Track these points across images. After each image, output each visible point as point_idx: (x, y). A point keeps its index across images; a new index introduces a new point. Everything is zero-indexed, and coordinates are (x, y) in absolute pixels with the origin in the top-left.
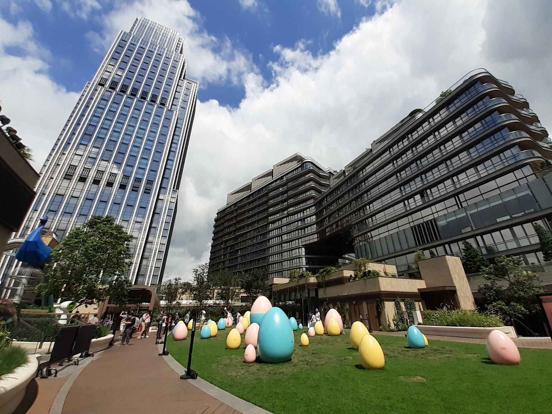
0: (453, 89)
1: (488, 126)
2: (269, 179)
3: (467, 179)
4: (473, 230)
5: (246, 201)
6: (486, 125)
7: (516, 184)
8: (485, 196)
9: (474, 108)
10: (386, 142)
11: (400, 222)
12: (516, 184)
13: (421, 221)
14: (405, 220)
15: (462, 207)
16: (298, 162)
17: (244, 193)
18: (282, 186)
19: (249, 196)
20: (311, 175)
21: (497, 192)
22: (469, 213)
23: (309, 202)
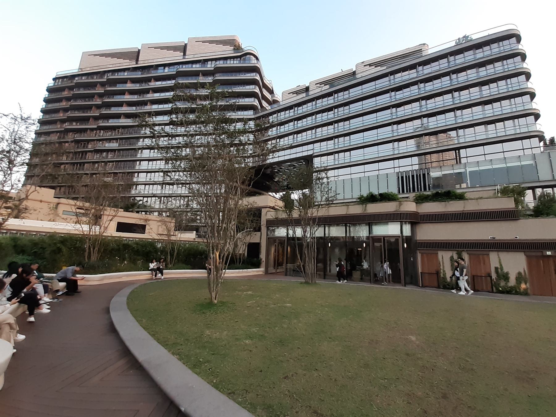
0: (474, 37)
1: (512, 87)
2: (178, 57)
3: (474, 135)
4: (468, 188)
5: (126, 75)
6: (510, 86)
7: (521, 153)
8: (488, 157)
9: (503, 63)
10: (379, 68)
11: (382, 165)
12: (521, 153)
13: (409, 168)
14: (390, 164)
15: (460, 162)
16: (234, 49)
17: (121, 61)
18: (206, 74)
19: (135, 69)
20: (258, 78)
21: (501, 156)
22: (469, 170)
23: (246, 113)
